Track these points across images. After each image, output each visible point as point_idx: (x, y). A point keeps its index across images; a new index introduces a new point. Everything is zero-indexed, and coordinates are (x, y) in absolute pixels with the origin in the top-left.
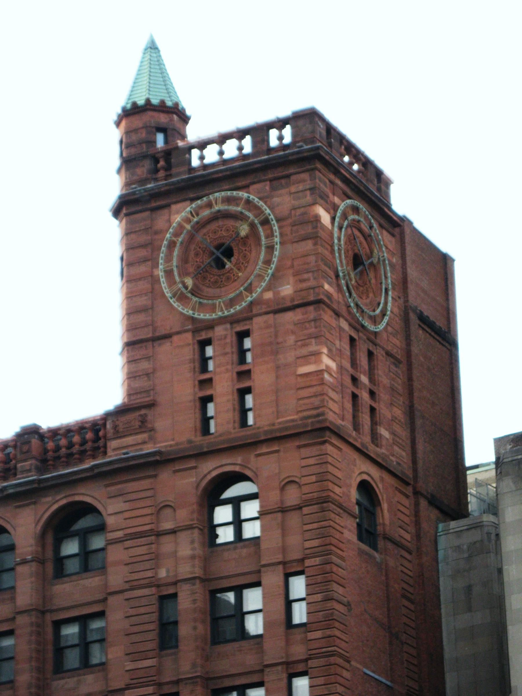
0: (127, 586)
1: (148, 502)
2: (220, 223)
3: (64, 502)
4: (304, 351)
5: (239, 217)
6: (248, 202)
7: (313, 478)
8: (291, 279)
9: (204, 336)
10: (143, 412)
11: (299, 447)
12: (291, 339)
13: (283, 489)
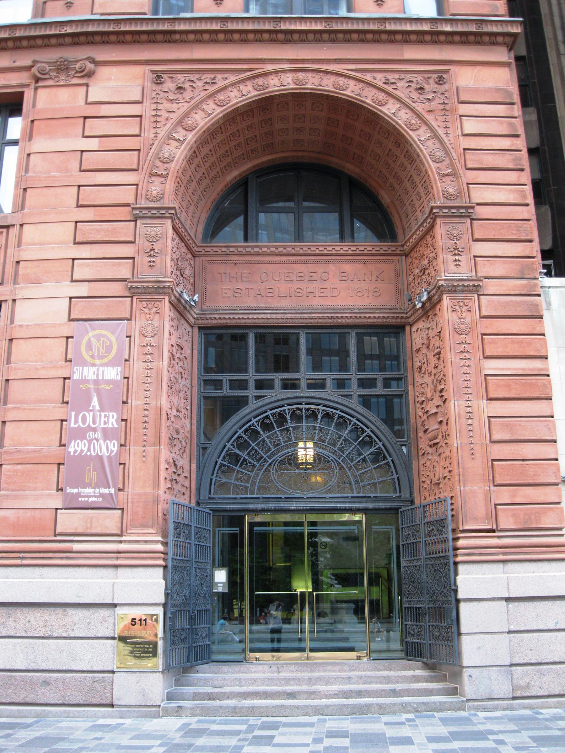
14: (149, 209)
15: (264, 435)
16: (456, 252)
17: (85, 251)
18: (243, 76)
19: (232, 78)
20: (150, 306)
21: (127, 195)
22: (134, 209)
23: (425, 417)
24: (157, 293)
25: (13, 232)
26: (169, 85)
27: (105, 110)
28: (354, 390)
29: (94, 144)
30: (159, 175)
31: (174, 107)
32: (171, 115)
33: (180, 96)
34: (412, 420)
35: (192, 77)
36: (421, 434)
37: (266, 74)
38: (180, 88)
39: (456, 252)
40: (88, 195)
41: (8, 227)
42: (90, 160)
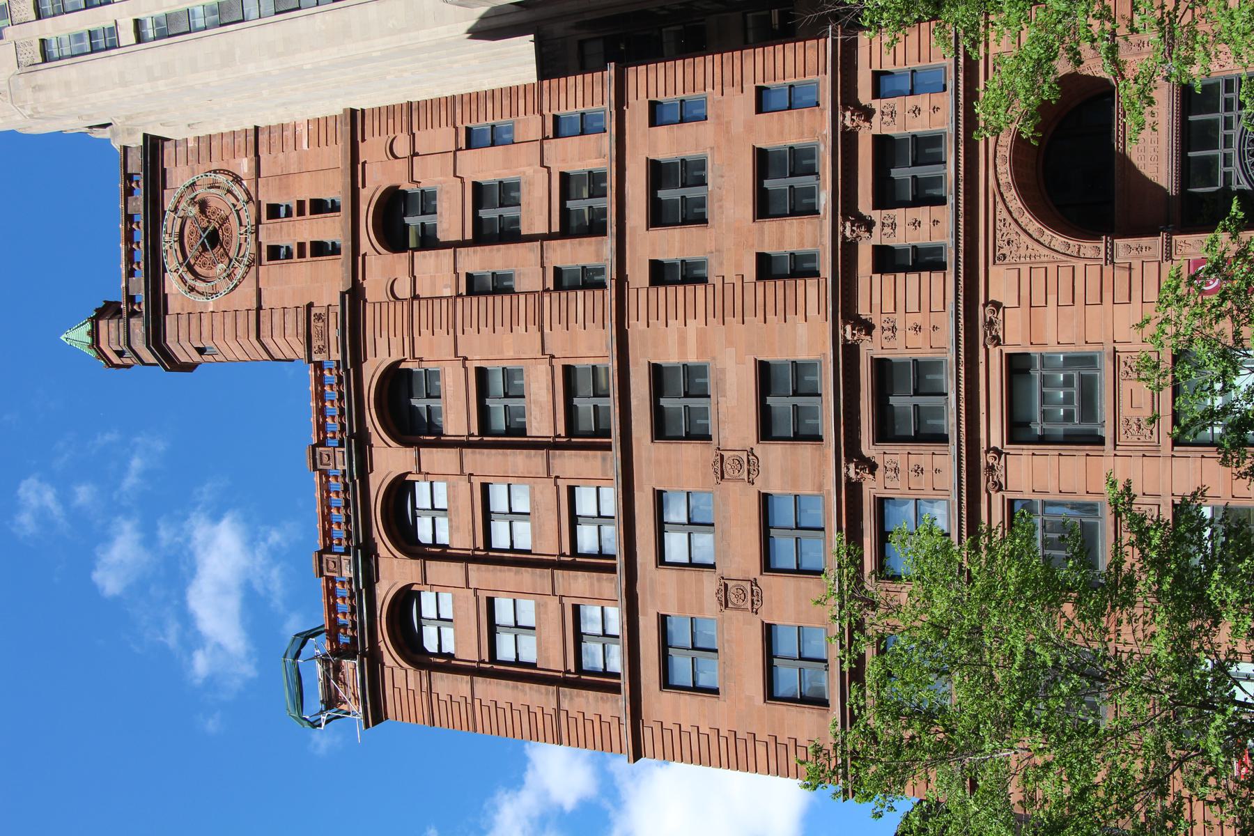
0: (451, 331)
1: (385, 306)
2: (186, 241)
3: (373, 411)
4: (291, 142)
6: (176, 210)
7: (391, 121)
8: (237, 161)
9: (264, 254)
10: (313, 318)
11: (363, 140)
12: (281, 155)
13: (396, 157)
14: (1106, 253)
17: (1136, 294)
18: (998, 198)
19: (1000, 206)
20: (1179, 247)
21: (1094, 271)
22: (1106, 265)
25: (1118, 347)
26: (1005, 250)
28: (1233, 114)
29: (1052, 298)
30: (1079, 251)
31: (1023, 246)
32: (1030, 247)
33: (1015, 241)
37: (998, 185)
39: (1141, 45)
40: (1093, 297)
41: (1115, 351)
42: (1065, 298)
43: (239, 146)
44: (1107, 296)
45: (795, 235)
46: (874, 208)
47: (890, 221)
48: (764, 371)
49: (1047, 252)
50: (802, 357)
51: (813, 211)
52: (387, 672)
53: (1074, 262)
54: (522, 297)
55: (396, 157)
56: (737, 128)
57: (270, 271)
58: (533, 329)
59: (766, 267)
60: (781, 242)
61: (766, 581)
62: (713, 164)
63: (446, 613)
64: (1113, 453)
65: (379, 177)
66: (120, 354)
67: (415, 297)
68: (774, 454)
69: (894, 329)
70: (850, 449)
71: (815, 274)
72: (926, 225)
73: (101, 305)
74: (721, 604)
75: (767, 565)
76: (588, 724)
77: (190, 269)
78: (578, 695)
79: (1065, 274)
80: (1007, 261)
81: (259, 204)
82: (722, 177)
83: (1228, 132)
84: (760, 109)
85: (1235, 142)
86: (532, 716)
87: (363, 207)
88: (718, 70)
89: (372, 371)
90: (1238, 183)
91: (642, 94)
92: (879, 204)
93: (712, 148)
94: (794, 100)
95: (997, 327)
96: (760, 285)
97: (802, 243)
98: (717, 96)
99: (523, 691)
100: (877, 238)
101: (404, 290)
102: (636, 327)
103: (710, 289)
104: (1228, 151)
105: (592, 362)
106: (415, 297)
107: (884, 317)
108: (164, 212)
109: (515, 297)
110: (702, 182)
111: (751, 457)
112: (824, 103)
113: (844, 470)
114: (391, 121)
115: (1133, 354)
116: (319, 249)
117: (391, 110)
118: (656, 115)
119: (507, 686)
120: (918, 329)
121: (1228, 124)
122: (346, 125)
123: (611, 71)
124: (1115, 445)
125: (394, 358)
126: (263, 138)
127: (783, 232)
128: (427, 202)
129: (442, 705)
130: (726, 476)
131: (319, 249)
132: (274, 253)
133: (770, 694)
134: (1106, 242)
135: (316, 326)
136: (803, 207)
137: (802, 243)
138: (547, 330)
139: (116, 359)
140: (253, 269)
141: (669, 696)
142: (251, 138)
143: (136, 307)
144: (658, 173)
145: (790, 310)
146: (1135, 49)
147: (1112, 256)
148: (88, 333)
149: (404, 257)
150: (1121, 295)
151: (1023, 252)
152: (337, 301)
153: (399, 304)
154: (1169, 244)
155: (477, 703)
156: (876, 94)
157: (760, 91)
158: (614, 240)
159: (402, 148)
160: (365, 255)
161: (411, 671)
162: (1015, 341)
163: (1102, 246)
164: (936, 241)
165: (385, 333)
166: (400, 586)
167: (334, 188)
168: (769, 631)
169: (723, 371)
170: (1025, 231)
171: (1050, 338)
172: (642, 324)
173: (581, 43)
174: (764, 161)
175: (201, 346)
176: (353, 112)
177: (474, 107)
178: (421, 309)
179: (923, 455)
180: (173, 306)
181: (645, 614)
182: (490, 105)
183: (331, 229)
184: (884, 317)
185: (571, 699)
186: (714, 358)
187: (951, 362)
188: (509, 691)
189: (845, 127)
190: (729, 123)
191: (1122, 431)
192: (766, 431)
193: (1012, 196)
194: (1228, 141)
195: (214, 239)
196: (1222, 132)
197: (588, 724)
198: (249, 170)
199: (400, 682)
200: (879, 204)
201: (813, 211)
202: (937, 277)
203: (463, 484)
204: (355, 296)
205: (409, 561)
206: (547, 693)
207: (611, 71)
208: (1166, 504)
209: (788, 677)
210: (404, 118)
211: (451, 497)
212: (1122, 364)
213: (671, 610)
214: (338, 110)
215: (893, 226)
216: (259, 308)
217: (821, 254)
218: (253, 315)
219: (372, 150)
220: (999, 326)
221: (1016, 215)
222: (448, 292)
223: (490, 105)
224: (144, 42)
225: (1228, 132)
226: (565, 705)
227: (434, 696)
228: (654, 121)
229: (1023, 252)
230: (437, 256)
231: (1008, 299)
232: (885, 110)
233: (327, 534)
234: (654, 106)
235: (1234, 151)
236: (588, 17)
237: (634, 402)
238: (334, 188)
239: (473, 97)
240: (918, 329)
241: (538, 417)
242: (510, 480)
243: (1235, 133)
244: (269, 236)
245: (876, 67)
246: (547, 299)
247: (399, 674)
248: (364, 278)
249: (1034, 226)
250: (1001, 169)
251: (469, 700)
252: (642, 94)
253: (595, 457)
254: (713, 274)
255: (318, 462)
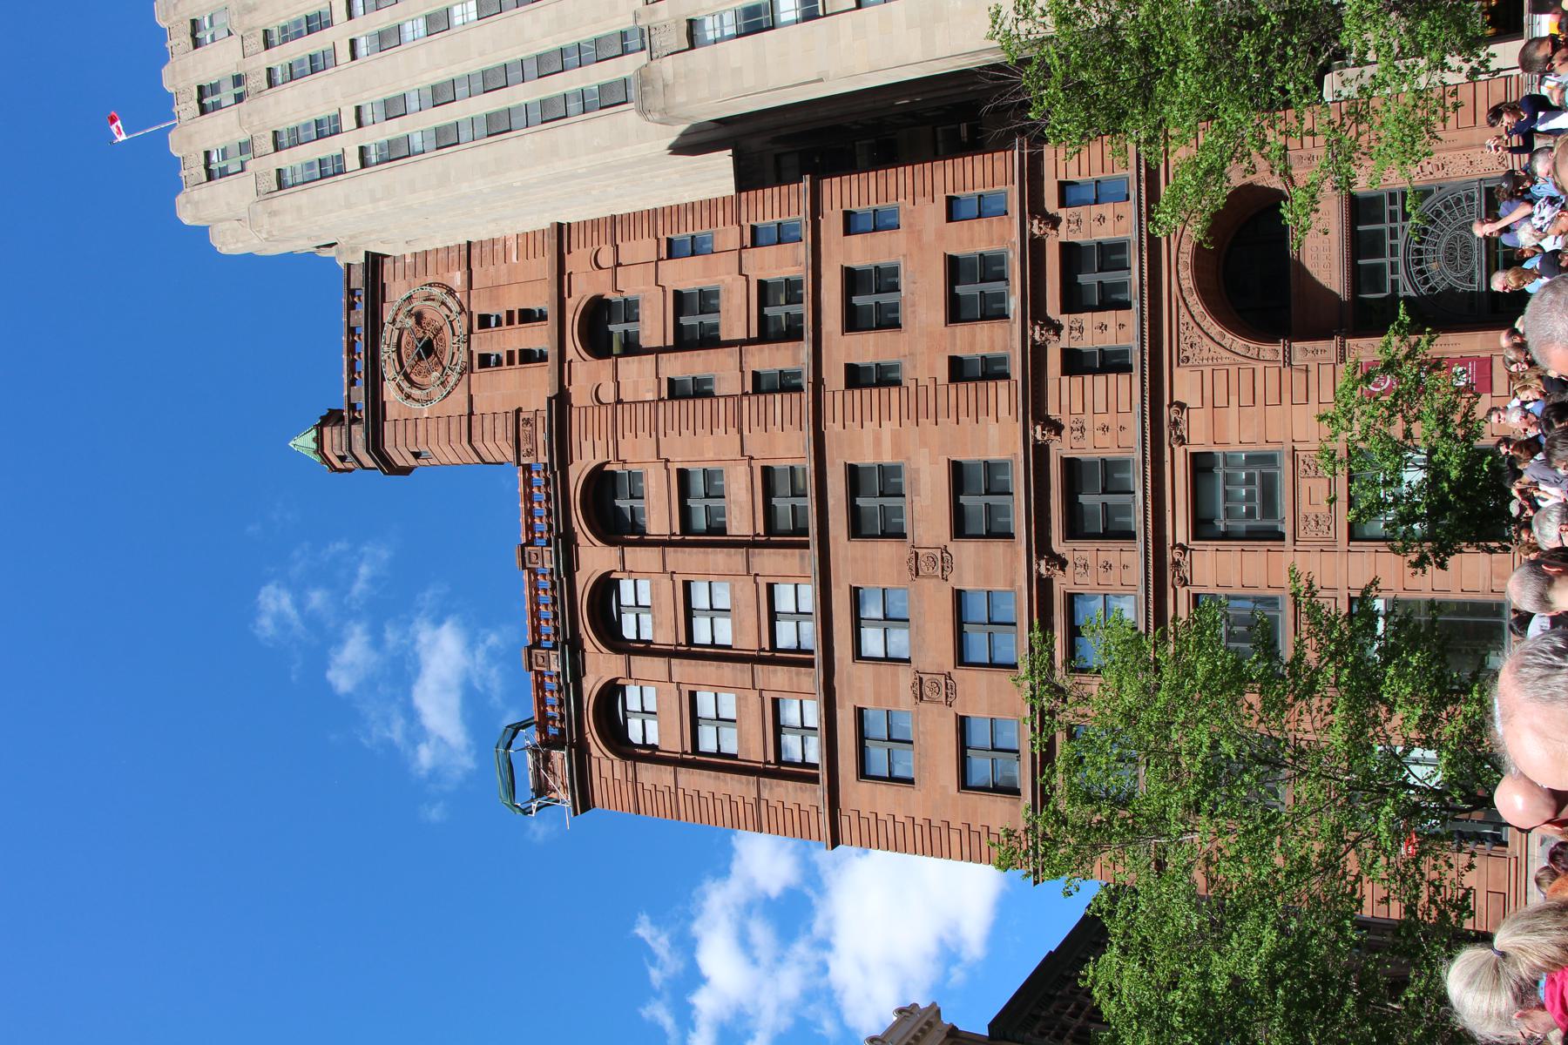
0: (654, 434)
1: (590, 411)
2: (403, 351)
3: (579, 512)
5: (401, 331)
6: (394, 322)
7: (595, 234)
8: (450, 274)
9: (476, 362)
10: (521, 423)
11: (569, 252)
13: (600, 268)
14: (1284, 356)
15: (1432, 283)
16: (1311, 158)
18: (1181, 303)
19: (1183, 310)
21: (1273, 374)
23: (1421, 174)
24: (1344, 346)
26: (1189, 353)
27: (1208, 393)
28: (1398, 225)
29: (1234, 399)
31: (1205, 349)
34: (1421, 184)
35: (1182, 339)
36: (1432, 177)
38: (1191, 346)
40: (1272, 397)
41: (1294, 450)
42: (1245, 401)
43: (453, 261)
44: (1286, 397)
45: (986, 339)
46: (1062, 313)
47: (1077, 325)
48: (958, 474)
49: (1228, 354)
50: (994, 456)
51: (1003, 315)
52: (594, 763)
53: (1254, 364)
54: (722, 401)
55: (600, 268)
56: (929, 236)
57: (480, 377)
58: (733, 431)
59: (959, 370)
60: (972, 345)
61: (961, 675)
62: (906, 271)
63: (651, 706)
64: (1293, 548)
65: (584, 288)
66: (342, 459)
67: (619, 401)
68: (967, 551)
69: (1082, 429)
70: (1041, 545)
71: (1005, 376)
72: (1111, 330)
73: (325, 413)
74: (916, 697)
75: (961, 660)
76: (788, 813)
77: (407, 377)
78: (778, 785)
79: (1246, 376)
80: (1190, 363)
81: (471, 314)
82: (915, 283)
83: (1394, 242)
84: (950, 218)
85: (1401, 251)
86: (734, 805)
87: (569, 316)
88: (909, 181)
89: (578, 472)
90: (1405, 290)
91: (837, 204)
92: (1067, 308)
93: (904, 256)
94: (984, 209)
95: (1181, 427)
96: (952, 387)
97: (993, 347)
98: (908, 204)
99: (725, 781)
100: (1065, 341)
101: (608, 395)
102: (832, 429)
103: (904, 391)
104: (1394, 259)
105: (790, 463)
106: (619, 401)
107: (1073, 418)
108: (383, 324)
109: (715, 400)
110: (895, 288)
111: (945, 555)
112: (1013, 211)
113: (1035, 567)
114: (595, 234)
115: (1310, 453)
116: (528, 356)
117: (595, 224)
118: (850, 224)
119: (709, 776)
120: (1105, 429)
121: (1393, 234)
122: (553, 238)
123: (806, 182)
124: (1295, 541)
125: (599, 460)
126: (475, 252)
127: (974, 336)
128: (630, 310)
129: (647, 794)
130: (921, 573)
131: (528, 356)
132: (485, 361)
133: (964, 784)
134: (1284, 345)
135: (525, 430)
136: (993, 311)
137: (992, 347)
138: (746, 432)
139: (338, 464)
140: (466, 376)
141: (866, 786)
142: (464, 252)
143: (356, 414)
144: (853, 280)
145: (982, 411)
146: (1306, 162)
147: (1290, 358)
148: (314, 440)
149: (609, 362)
150: (1299, 395)
151: (1205, 354)
152: (545, 406)
153: (603, 409)
154: (1343, 347)
155: (680, 792)
156: (1063, 203)
157: (950, 201)
158: (811, 345)
159: (606, 259)
160: (570, 362)
161: (617, 762)
162: (1199, 440)
163: (1280, 349)
164: (1122, 344)
165: (590, 437)
166: (605, 680)
167: (542, 299)
168: (962, 723)
169: (917, 471)
170: (1207, 335)
171: (1233, 437)
172: (838, 426)
173: (778, 158)
174: (955, 268)
175: (417, 450)
176: (560, 226)
177: (675, 219)
178: (625, 414)
179: (1111, 552)
180: (391, 413)
181: (842, 707)
182: (690, 217)
183: (539, 337)
184: (1073, 418)
185: (771, 789)
186: (908, 459)
187: (1138, 461)
188: (712, 781)
189: (1032, 235)
190: (920, 231)
191: (1301, 528)
192: (960, 529)
193: (1194, 301)
194: (1394, 253)
195: (428, 349)
196: (1388, 242)
197: (788, 813)
198: (462, 282)
199: (606, 772)
200: (1067, 308)
201: (1003, 315)
202: (1123, 379)
203: (665, 582)
204: (561, 401)
205: (614, 656)
206: (748, 783)
207: (806, 182)
208: (1342, 597)
209: (981, 769)
210: (608, 230)
211: (654, 595)
212: (1301, 463)
213: (867, 704)
214: (546, 225)
215: (1081, 329)
216: (471, 414)
217: (1012, 357)
218: (465, 420)
219: (577, 261)
220: (1183, 426)
221: (1198, 319)
222: (650, 396)
223: (690, 217)
224: (368, 167)
225: (1394, 242)
226: (765, 794)
227: (639, 786)
228: (847, 231)
229: (1205, 354)
230: (640, 362)
231: (1192, 400)
232: (1071, 219)
233: (536, 630)
234: (848, 215)
235: (1400, 259)
236: (784, 132)
237: (831, 502)
238: (542, 299)
239: (675, 209)
240: (1105, 429)
241: (738, 516)
242: (711, 578)
243: (1400, 242)
244: (480, 344)
245: (1062, 177)
246: (745, 403)
247: (606, 764)
248: (570, 384)
249: (1215, 329)
250: (1183, 275)
251: (673, 790)
252: (837, 204)
253: (793, 555)
254: (907, 378)
255: (527, 561)
